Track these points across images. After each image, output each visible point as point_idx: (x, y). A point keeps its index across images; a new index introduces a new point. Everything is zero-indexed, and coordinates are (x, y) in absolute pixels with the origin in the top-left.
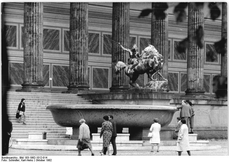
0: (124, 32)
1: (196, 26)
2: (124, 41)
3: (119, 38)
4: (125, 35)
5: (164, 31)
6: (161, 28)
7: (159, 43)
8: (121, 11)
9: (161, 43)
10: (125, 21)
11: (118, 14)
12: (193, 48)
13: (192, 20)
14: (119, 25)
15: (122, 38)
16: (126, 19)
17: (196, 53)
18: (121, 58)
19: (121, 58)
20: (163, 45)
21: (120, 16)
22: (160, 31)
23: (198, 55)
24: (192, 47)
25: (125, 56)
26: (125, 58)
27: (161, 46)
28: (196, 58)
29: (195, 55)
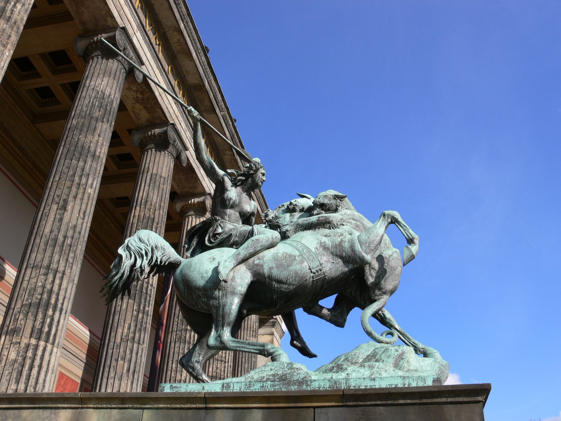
0: (70, 246)
1: (188, 335)
3: (51, 257)
4: (71, 255)
5: (147, 308)
6: (141, 298)
7: (131, 335)
8: (79, 184)
9: (137, 335)
10: (82, 215)
11: (66, 191)
14: (61, 220)
15: (62, 264)
16: (85, 213)
18: (43, 323)
19: (43, 323)
20: (139, 343)
21: (71, 198)
22: (139, 306)
25: (59, 321)
26: (57, 330)
27: (136, 345)
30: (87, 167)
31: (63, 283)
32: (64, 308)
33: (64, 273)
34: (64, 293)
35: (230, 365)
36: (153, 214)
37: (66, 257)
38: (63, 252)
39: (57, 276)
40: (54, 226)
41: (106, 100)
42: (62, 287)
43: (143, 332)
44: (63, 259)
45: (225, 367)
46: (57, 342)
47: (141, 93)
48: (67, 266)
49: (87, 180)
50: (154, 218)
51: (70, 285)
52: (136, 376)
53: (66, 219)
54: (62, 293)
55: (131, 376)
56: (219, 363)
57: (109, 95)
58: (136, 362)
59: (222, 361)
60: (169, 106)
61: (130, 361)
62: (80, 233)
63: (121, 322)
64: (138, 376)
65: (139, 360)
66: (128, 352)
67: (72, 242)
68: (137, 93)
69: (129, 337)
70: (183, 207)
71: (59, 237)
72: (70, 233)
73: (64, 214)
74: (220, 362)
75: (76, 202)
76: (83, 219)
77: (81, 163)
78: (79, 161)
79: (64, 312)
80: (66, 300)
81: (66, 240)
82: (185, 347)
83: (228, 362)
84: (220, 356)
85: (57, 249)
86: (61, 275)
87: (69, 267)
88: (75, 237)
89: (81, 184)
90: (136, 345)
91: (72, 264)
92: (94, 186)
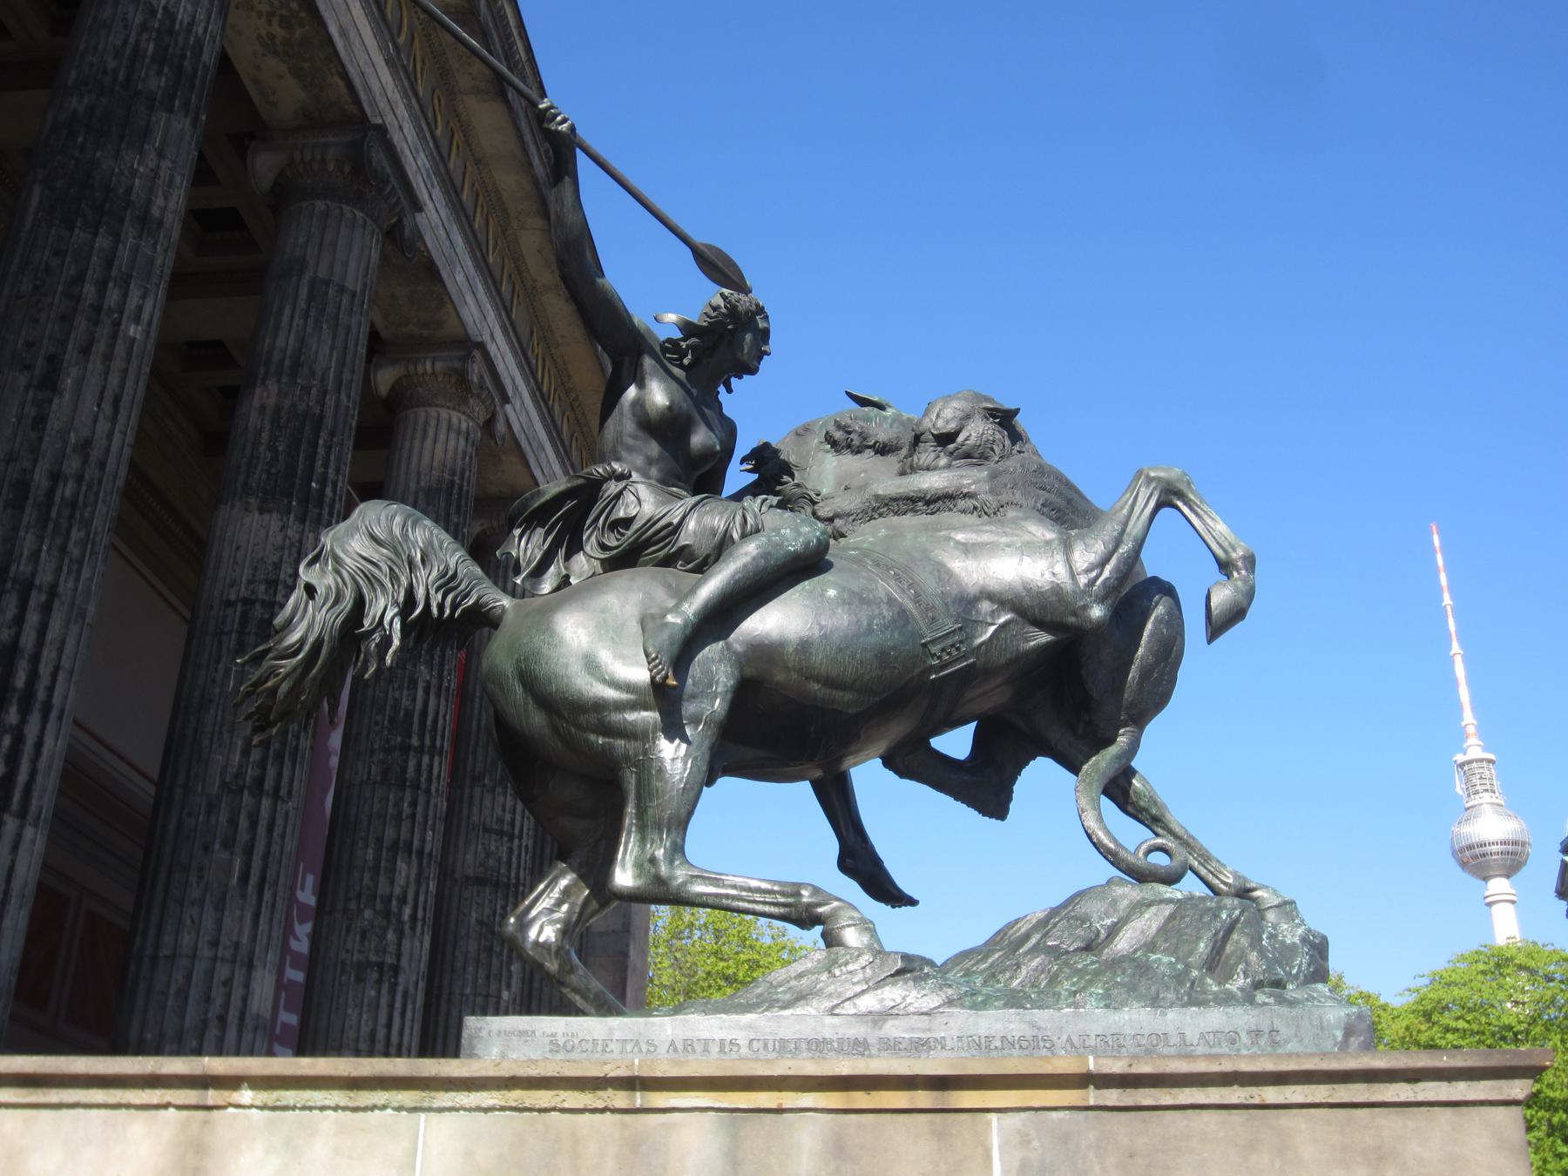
1: (412, 764)
2: (61, 589)
4: (76, 534)
7: (251, 772)
9: (271, 773)
10: (107, 407)
12: (379, 906)
13: (392, 720)
14: (40, 421)
17: (392, 949)
20: (276, 795)
21: (71, 353)
23: (404, 962)
24: (374, 897)
25: (39, 745)
26: (33, 773)
27: (266, 803)
28: (392, 992)
29: (389, 960)
30: (124, 252)
31: (52, 623)
32: (56, 700)
33: (53, 592)
34: (54, 655)
35: (527, 845)
36: (318, 402)
37: (58, 541)
38: (51, 526)
39: (32, 602)
40: (18, 439)
41: (181, 39)
42: (50, 636)
43: (287, 764)
44: (49, 551)
45: (511, 850)
46: (33, 809)
47: (286, 23)
48: (65, 569)
49: (125, 296)
50: (321, 417)
51: (75, 630)
52: (267, 895)
53: (58, 419)
54: (48, 654)
55: (254, 898)
56: (496, 841)
57: (191, 25)
58: (266, 855)
59: (501, 833)
60: (369, 71)
61: (249, 851)
62: (102, 465)
63: (221, 733)
64: (275, 896)
65: (275, 848)
66: (243, 823)
67: (77, 494)
68: (270, 23)
69: (248, 779)
70: (398, 381)
71: (36, 476)
72: (72, 465)
73: (50, 402)
74: (498, 837)
75: (90, 366)
76: (114, 419)
77: (103, 242)
78: (95, 234)
79: (54, 714)
80: (61, 678)
81: (61, 487)
82: (402, 799)
83: (521, 838)
84: (497, 819)
85: (29, 515)
86: (43, 598)
87: (70, 571)
88: (87, 477)
89: (106, 307)
90: (266, 803)
91: (80, 563)
92: (145, 316)
